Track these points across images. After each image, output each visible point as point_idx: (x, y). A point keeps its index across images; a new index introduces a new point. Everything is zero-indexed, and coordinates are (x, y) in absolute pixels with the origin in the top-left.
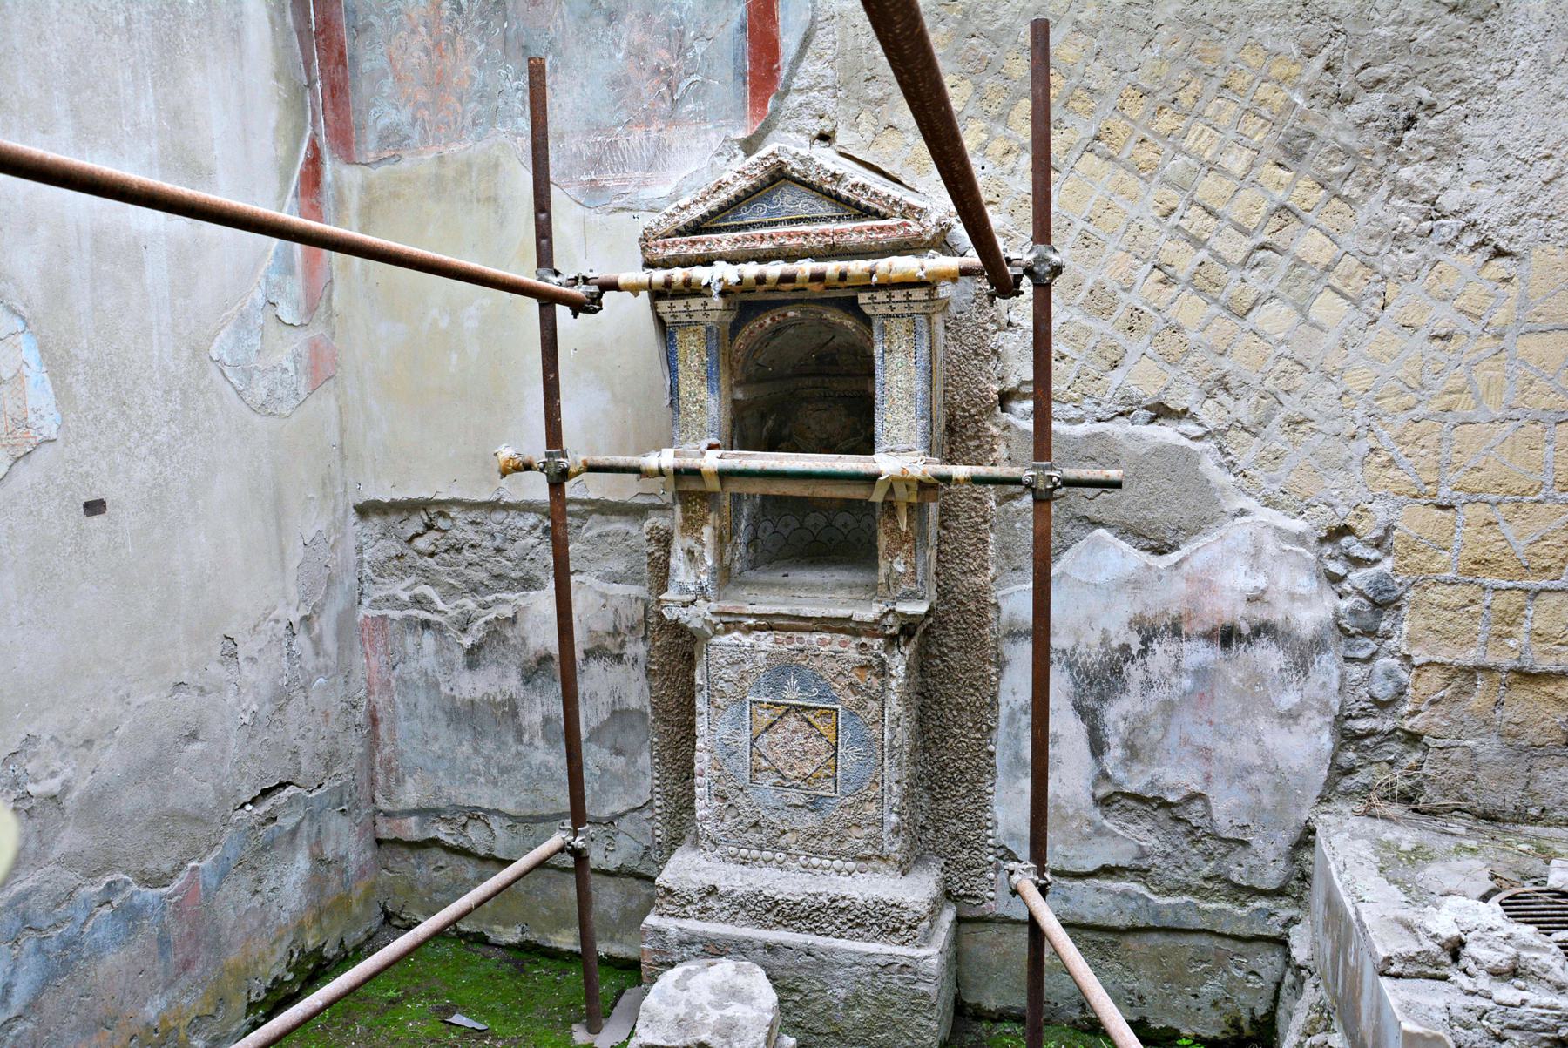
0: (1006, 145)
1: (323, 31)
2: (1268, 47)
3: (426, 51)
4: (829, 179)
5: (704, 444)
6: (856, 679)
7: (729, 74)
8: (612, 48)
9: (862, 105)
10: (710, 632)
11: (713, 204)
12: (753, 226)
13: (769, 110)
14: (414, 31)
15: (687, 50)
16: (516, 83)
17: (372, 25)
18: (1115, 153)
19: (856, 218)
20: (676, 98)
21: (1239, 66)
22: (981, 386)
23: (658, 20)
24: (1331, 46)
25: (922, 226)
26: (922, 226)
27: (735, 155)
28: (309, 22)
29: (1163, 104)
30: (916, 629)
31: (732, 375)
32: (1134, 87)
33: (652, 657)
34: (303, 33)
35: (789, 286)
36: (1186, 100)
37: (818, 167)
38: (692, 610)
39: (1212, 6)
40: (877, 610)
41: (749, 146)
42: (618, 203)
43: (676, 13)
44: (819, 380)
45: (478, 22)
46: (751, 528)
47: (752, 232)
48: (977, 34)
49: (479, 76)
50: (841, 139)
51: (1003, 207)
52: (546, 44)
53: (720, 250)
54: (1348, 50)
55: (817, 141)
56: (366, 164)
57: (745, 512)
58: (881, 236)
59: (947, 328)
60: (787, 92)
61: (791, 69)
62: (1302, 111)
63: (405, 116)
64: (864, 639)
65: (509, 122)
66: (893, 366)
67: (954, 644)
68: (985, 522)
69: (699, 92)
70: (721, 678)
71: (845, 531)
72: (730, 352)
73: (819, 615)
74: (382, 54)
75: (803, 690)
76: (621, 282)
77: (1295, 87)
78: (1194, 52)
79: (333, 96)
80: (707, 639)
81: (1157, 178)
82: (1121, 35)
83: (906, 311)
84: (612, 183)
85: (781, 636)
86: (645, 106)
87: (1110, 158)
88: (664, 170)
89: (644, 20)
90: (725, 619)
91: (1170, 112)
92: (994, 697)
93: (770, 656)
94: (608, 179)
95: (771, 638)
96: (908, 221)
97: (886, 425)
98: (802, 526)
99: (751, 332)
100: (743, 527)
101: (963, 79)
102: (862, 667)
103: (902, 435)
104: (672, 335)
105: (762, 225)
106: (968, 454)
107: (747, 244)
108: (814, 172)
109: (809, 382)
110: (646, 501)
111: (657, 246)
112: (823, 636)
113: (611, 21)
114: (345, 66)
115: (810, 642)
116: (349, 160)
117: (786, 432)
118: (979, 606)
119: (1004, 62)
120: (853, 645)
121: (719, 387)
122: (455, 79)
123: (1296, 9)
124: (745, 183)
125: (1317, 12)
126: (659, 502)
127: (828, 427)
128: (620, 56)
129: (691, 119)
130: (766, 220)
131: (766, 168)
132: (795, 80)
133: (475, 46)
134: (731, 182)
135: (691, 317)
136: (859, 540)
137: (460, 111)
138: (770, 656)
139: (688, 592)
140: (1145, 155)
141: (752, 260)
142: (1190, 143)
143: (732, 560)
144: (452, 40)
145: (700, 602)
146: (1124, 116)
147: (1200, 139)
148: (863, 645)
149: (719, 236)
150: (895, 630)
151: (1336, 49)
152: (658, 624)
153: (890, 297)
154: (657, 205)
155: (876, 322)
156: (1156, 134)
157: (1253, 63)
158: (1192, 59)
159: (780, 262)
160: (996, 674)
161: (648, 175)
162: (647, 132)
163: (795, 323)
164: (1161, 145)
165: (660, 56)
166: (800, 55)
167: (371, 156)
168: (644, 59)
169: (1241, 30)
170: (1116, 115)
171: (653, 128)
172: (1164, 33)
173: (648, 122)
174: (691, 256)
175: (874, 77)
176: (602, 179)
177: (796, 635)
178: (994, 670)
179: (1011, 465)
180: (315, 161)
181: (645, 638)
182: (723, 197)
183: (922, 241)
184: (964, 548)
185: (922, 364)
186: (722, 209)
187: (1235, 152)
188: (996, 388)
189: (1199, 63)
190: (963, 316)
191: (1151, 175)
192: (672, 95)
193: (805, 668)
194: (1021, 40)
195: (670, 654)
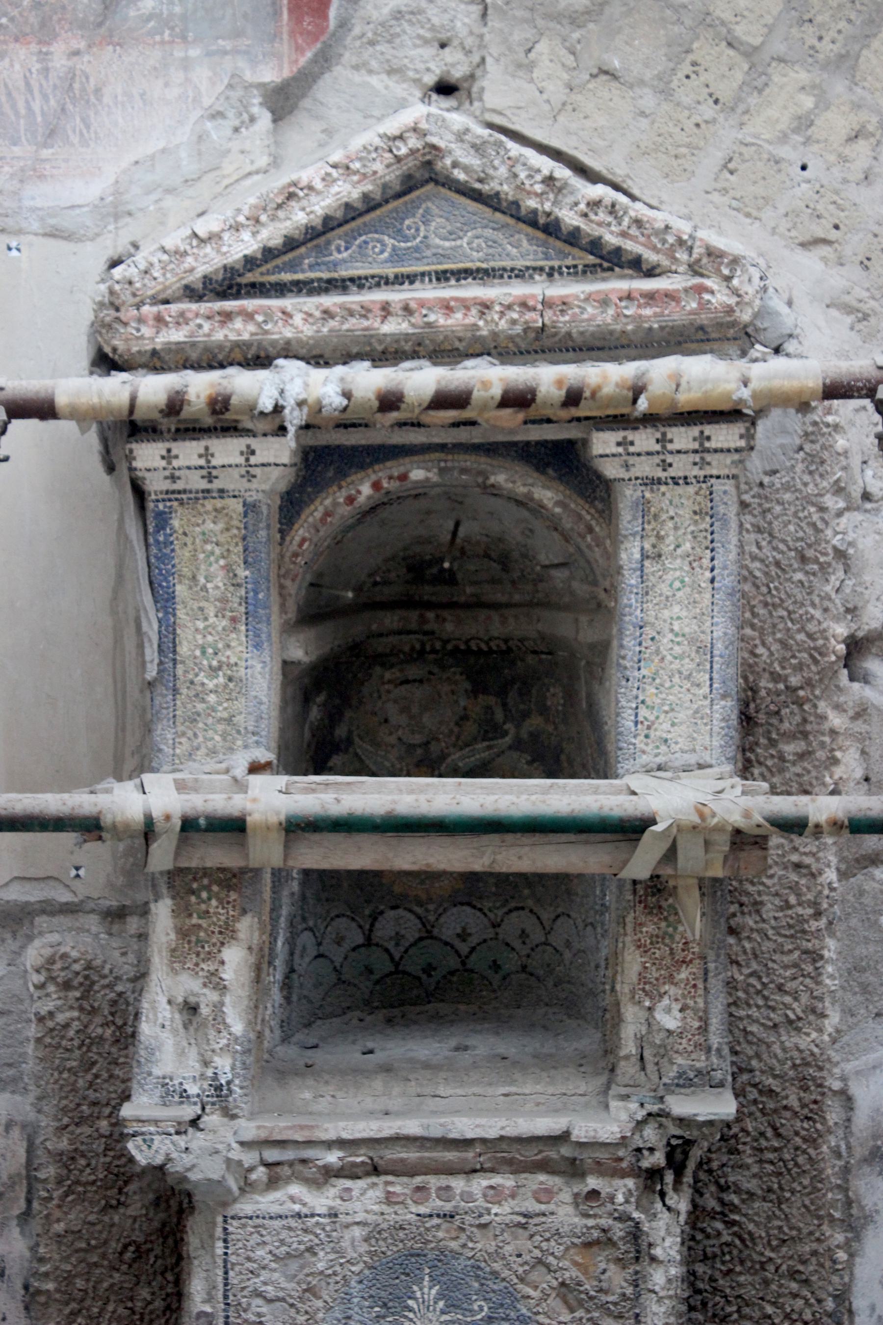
0: (854, 121)
4: (538, 188)
5: (240, 762)
6: (574, 1273)
9: (540, 22)
10: (234, 1188)
12: (358, 283)
19: (589, 271)
22: (811, 627)
25: (736, 293)
26: (736, 293)
27: (252, 119)
30: (686, 1154)
31: (283, 607)
33: (41, 1260)
35: (451, 415)
37: (513, 162)
38: (197, 1140)
40: (624, 1116)
44: (414, 615)
46: (287, 946)
47: (354, 299)
53: (288, 333)
55: (434, 96)
57: (285, 911)
58: (648, 312)
59: (744, 505)
64: (593, 1182)
66: (664, 588)
67: (752, 1185)
68: (818, 914)
70: (258, 1294)
71: (464, 949)
72: (282, 556)
73: (492, 1133)
75: (452, 1306)
76: (62, 400)
80: (225, 1204)
83: (696, 471)
85: (400, 1186)
88: (84, 143)
90: (272, 1155)
92: (842, 1297)
93: (374, 1234)
95: (377, 1193)
96: (708, 283)
97: (643, 712)
98: (369, 942)
99: (327, 514)
100: (280, 943)
102: (588, 1245)
103: (680, 736)
104: (163, 519)
105: (382, 282)
106: (781, 770)
107: (353, 323)
108: (503, 171)
109: (391, 620)
110: (33, 894)
111: (141, 320)
112: (497, 1180)
115: (467, 1197)
117: (341, 732)
118: (808, 1097)
120: (566, 1196)
121: (269, 635)
126: (65, 897)
127: (426, 719)
129: (151, 33)
130: (390, 271)
131: (398, 159)
134: (318, 185)
135: (210, 478)
136: (496, 966)
138: (374, 1234)
139: (184, 1095)
141: (360, 357)
143: (263, 1020)
145: (212, 1119)
148: (594, 1194)
149: (288, 303)
150: (659, 1158)
152: (60, 1182)
153: (663, 440)
154: (66, 222)
155: (628, 496)
159: (425, 363)
160: (847, 1245)
161: (46, 153)
162: (44, 56)
163: (419, 493)
171: (58, 49)
174: (221, 347)
177: (434, 1182)
178: (839, 1238)
179: (869, 793)
181: (26, 1216)
183: (733, 324)
184: (769, 971)
185: (727, 581)
186: (291, 244)
188: (841, 630)
190: (777, 480)
193: (456, 1255)
195: (90, 1249)
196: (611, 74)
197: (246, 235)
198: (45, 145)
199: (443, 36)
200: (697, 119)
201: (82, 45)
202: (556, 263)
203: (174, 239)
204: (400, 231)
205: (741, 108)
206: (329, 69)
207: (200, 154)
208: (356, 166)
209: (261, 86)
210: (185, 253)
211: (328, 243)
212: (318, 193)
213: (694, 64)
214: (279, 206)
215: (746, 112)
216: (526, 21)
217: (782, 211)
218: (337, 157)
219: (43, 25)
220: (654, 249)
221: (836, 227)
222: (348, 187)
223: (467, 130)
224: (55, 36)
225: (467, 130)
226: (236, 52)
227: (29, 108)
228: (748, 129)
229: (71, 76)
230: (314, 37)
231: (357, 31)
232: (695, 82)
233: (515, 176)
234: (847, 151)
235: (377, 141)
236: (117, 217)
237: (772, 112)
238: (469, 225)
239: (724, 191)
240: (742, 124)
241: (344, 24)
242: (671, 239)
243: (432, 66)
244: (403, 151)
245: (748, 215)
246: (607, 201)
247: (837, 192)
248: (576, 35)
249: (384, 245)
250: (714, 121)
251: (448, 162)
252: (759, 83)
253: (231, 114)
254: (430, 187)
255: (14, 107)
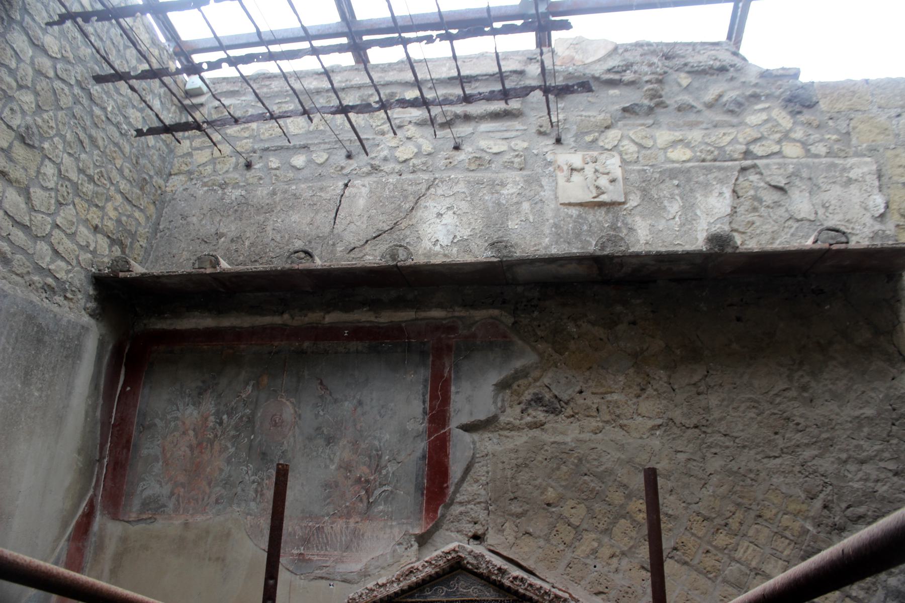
0: (611, 551)
1: (119, 425)
2: (784, 491)
3: (191, 448)
4: (496, 572)
7: (411, 488)
8: (328, 461)
9: (506, 516)
11: (404, 584)
13: (439, 515)
14: (185, 433)
15: (382, 468)
16: (253, 478)
17: (155, 425)
18: (688, 560)
20: (371, 500)
21: (766, 503)
23: (363, 446)
24: (824, 493)
27: (412, 546)
28: (111, 417)
29: (719, 527)
32: (698, 514)
34: (105, 424)
36: (734, 524)
37: (488, 562)
39: (744, 463)
41: (423, 540)
42: (319, 573)
43: (376, 443)
45: (233, 433)
48: (588, 474)
49: (227, 469)
50: (492, 539)
51: (611, 596)
52: (280, 453)
54: (835, 496)
55: (471, 540)
56: (128, 522)
60: (452, 503)
61: (456, 487)
62: (813, 536)
63: (166, 490)
65: (243, 505)
69: (389, 498)
74: (158, 445)
77: (806, 518)
78: (735, 493)
79: (114, 469)
81: (720, 579)
82: (686, 480)
84: (316, 558)
86: (348, 504)
87: (686, 563)
88: (357, 551)
89: (353, 445)
91: (724, 532)
94: (314, 555)
101: (579, 503)
108: (484, 565)
113: (329, 443)
114: (129, 450)
116: (115, 517)
119: (608, 493)
122: (208, 470)
123: (798, 468)
124: (430, 570)
125: (811, 470)
128: (333, 467)
129: (381, 517)
131: (448, 560)
132: (458, 495)
133: (227, 448)
134: (420, 568)
137: (207, 490)
140: (709, 562)
142: (740, 555)
144: (211, 442)
146: (693, 534)
147: (746, 551)
151: (828, 495)
154: (349, 577)
156: (716, 547)
157: (776, 502)
158: (734, 497)
161: (345, 554)
162: (347, 523)
164: (720, 555)
165: (362, 470)
166: (463, 479)
167: (133, 516)
168: (350, 471)
169: (764, 480)
170: (687, 533)
171: (352, 521)
172: (715, 479)
173: (348, 515)
175: (516, 498)
176: (309, 555)
180: (89, 515)
182: (414, 579)
186: (411, 588)
187: (773, 562)
189: (740, 500)
191: (716, 576)
192: (368, 498)
194: (618, 479)
196: (530, 534)
197: (395, 585)
198: (345, 552)
199: (476, 520)
200: (558, 549)
201: (359, 520)
202: (503, 599)
203: (370, 585)
204: (449, 586)
205: (573, 547)
206: (438, 530)
207: (394, 556)
208: (434, 562)
209: (415, 535)
210: (374, 590)
211: (424, 589)
212: (421, 571)
213: (557, 531)
214: (407, 575)
215: (575, 547)
216: (501, 516)
217: (588, 582)
218: (427, 559)
219: (348, 513)
220: (537, 595)
221: (607, 588)
222: (431, 569)
223: (472, 551)
224: (351, 517)
225: (472, 551)
226: (407, 523)
227: (341, 539)
228: (575, 553)
229: (355, 529)
230: (433, 519)
231: (448, 518)
232: (558, 537)
233: (488, 567)
234: (609, 561)
235: (441, 554)
236: (365, 576)
237: (583, 548)
238: (473, 584)
239: (568, 574)
240: (573, 552)
241: (443, 516)
242: (542, 592)
243: (472, 530)
244: (450, 557)
245: (576, 583)
246: (520, 577)
247: (607, 576)
248: (518, 521)
249: (443, 590)
250: (564, 550)
251: (465, 562)
252: (579, 538)
253: (405, 543)
254: (459, 570)
255: (336, 539)
